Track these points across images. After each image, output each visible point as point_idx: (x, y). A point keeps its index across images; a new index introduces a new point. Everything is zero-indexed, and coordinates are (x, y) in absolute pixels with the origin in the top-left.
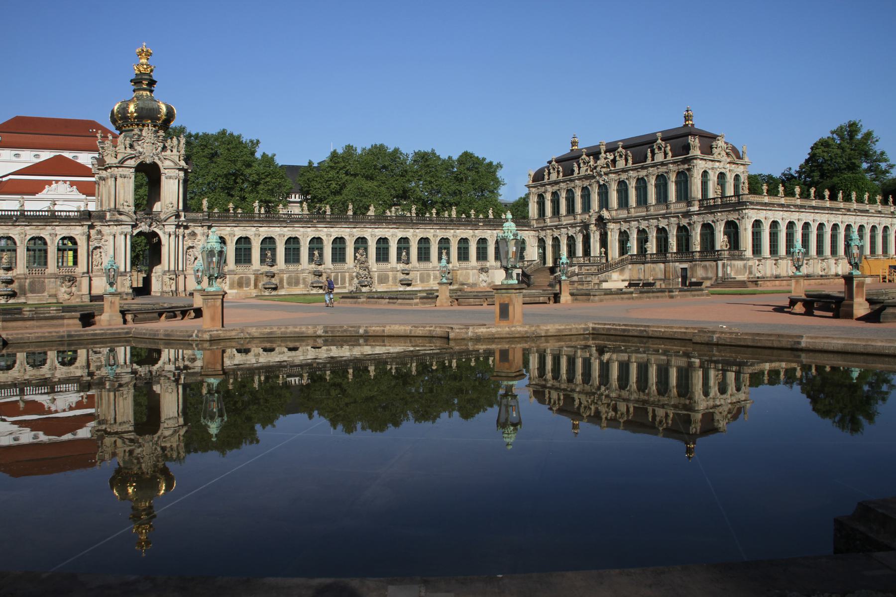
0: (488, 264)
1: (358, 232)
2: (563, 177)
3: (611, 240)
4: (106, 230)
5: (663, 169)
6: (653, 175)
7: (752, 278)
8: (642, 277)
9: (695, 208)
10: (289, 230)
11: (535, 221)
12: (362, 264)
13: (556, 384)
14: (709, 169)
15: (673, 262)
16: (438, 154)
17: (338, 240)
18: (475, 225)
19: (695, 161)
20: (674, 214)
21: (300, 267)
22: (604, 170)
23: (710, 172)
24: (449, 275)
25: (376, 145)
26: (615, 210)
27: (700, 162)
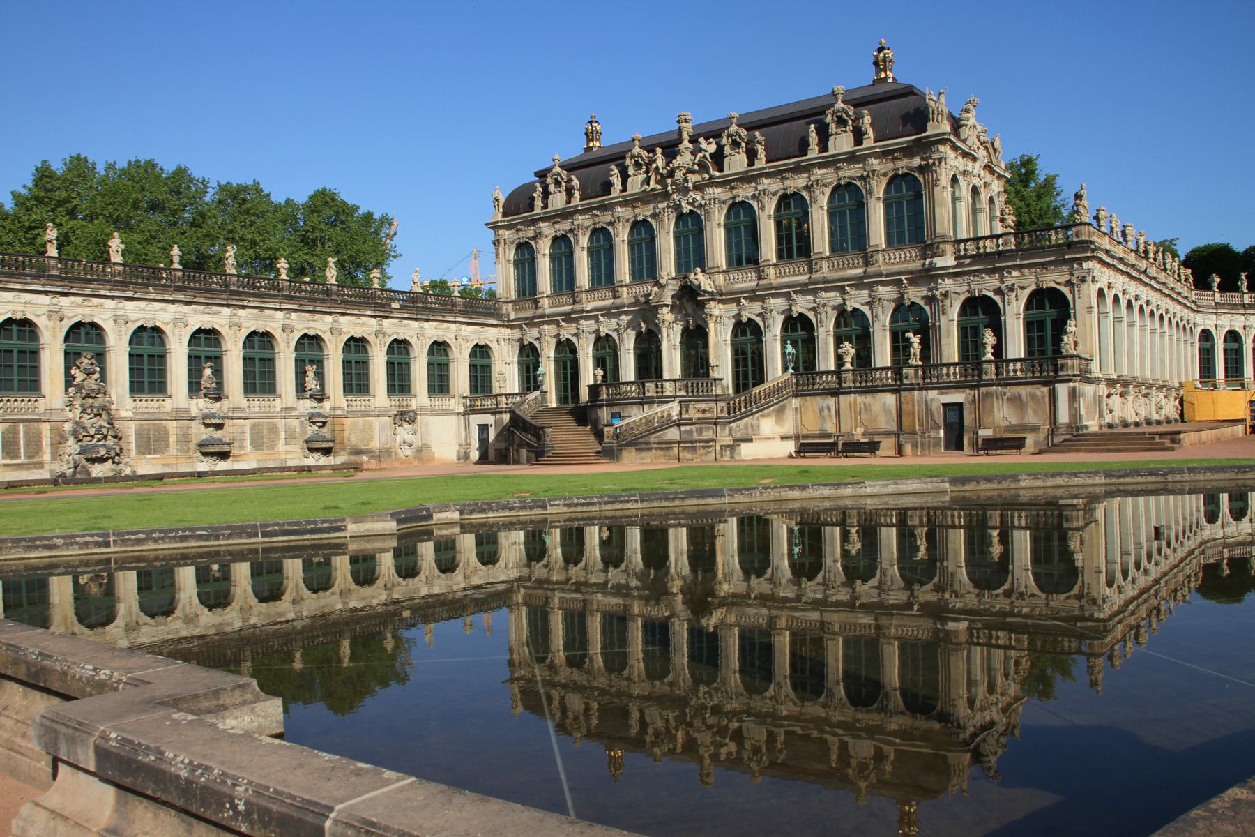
0: (414, 404)
1: (75, 309)
2: (581, 200)
3: (716, 344)
5: (850, 172)
6: (826, 185)
8: (830, 427)
11: (510, 305)
13: (577, 676)
15: (920, 389)
16: (266, 191)
18: (384, 306)
19: (941, 148)
20: (887, 275)
22: (693, 178)
24: (325, 430)
25: (138, 161)
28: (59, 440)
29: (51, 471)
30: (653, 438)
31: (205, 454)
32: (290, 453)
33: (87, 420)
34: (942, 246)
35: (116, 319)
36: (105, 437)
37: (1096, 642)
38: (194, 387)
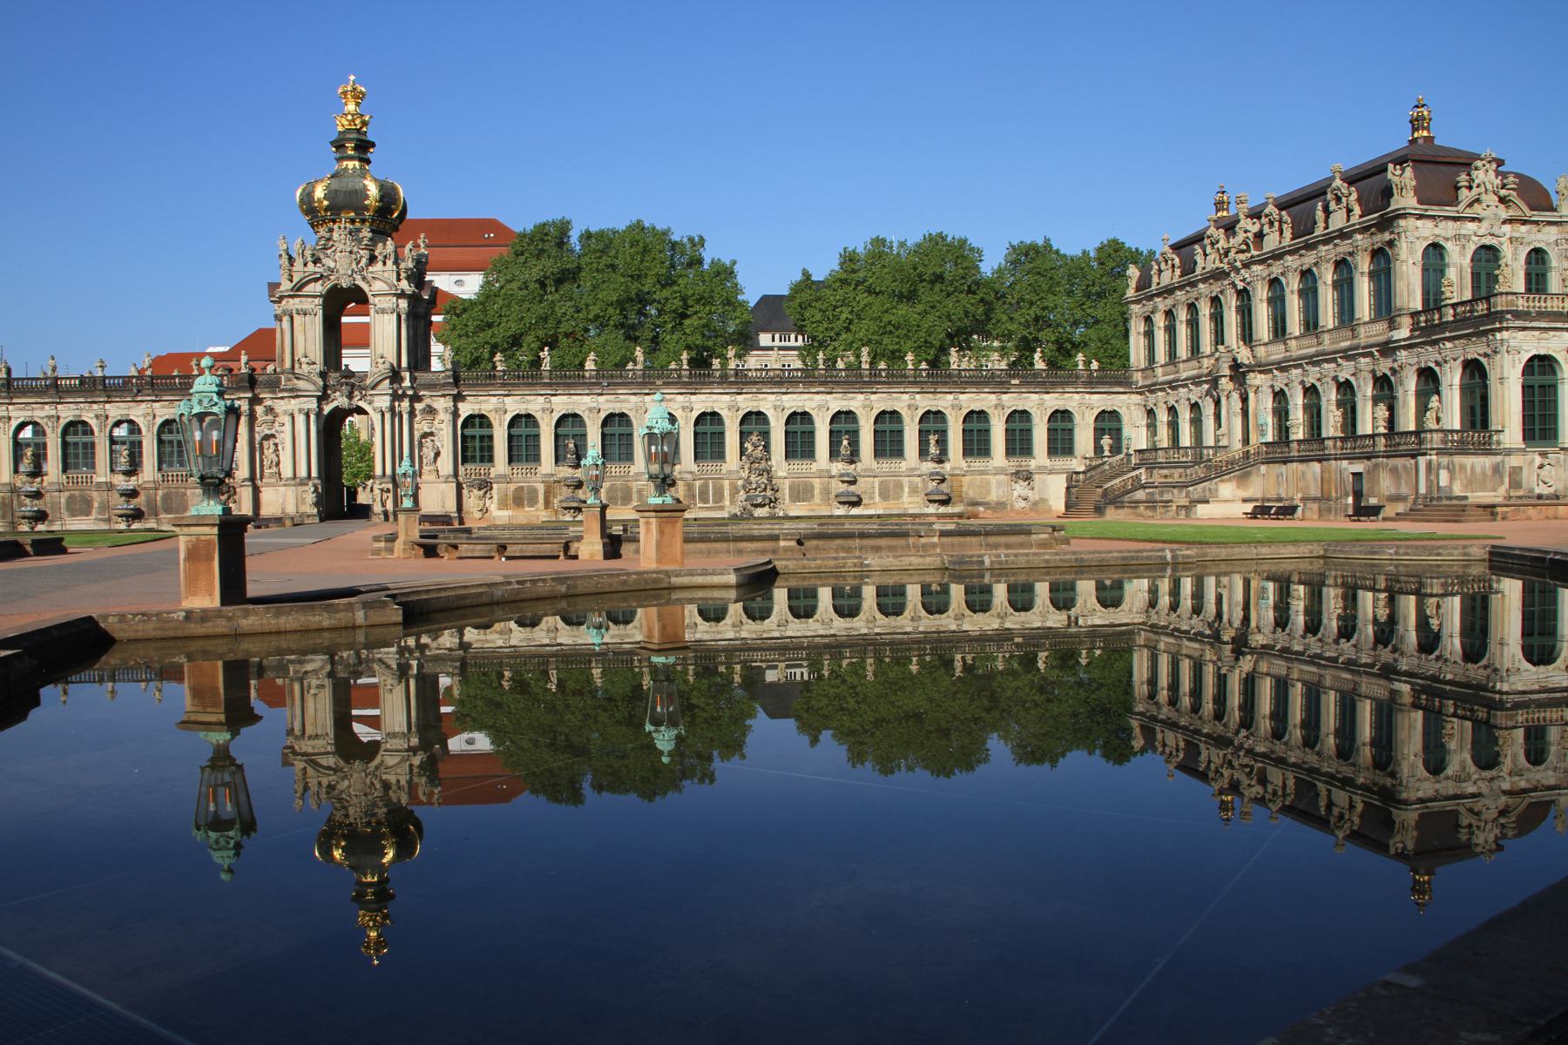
4: (281, 406)
7: (1520, 497)
9: (1403, 333)
10: (608, 401)
11: (1140, 373)
12: (758, 462)
14: (1447, 239)
15: (1336, 459)
17: (975, 415)
18: (1002, 383)
19: (1402, 223)
21: (634, 469)
23: (1448, 246)
24: (944, 485)
26: (1266, 344)
27: (1419, 223)
28: (734, 491)
29: (729, 512)
30: (1126, 498)
31: (840, 503)
32: (911, 503)
33: (753, 478)
34: (1398, 319)
35: (775, 408)
36: (765, 490)
37: (1499, 713)
38: (834, 454)
